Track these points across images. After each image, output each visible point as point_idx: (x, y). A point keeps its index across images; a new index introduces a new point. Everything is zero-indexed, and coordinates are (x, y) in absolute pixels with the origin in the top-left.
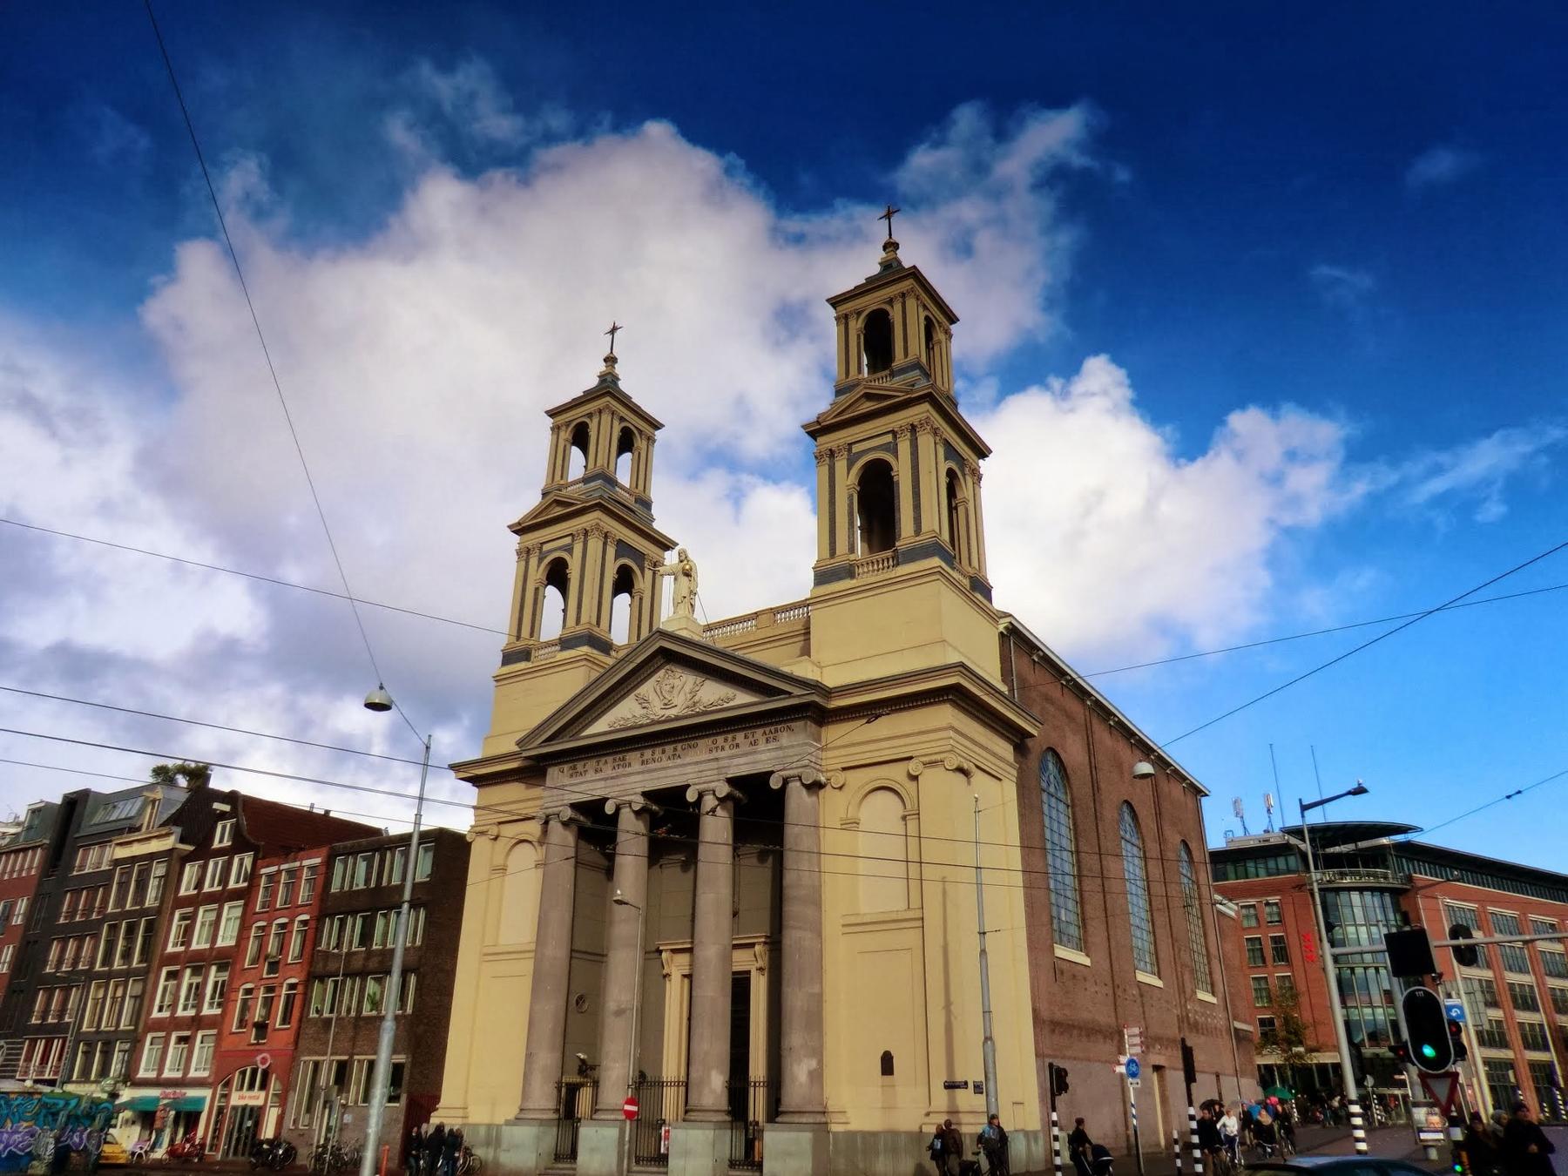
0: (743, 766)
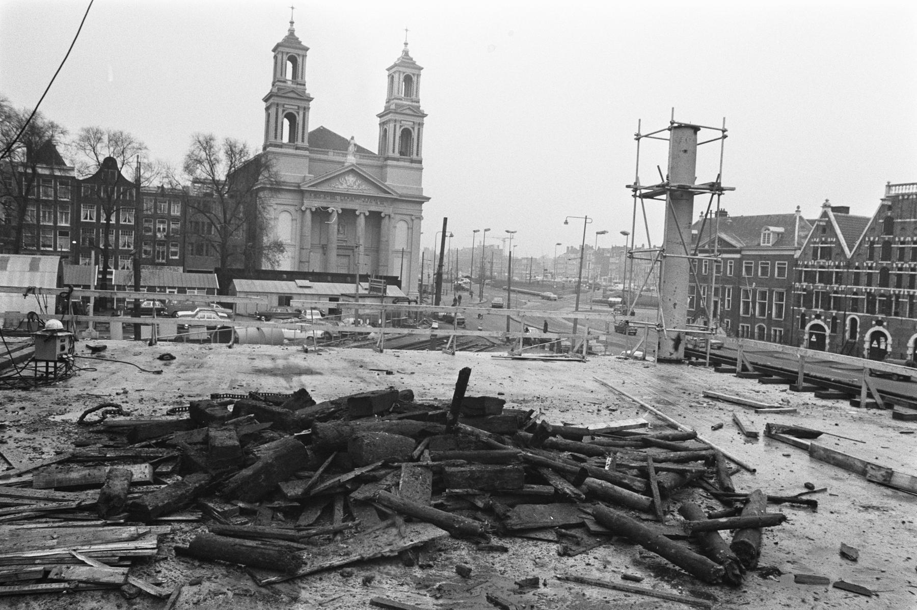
0: (374, 208)
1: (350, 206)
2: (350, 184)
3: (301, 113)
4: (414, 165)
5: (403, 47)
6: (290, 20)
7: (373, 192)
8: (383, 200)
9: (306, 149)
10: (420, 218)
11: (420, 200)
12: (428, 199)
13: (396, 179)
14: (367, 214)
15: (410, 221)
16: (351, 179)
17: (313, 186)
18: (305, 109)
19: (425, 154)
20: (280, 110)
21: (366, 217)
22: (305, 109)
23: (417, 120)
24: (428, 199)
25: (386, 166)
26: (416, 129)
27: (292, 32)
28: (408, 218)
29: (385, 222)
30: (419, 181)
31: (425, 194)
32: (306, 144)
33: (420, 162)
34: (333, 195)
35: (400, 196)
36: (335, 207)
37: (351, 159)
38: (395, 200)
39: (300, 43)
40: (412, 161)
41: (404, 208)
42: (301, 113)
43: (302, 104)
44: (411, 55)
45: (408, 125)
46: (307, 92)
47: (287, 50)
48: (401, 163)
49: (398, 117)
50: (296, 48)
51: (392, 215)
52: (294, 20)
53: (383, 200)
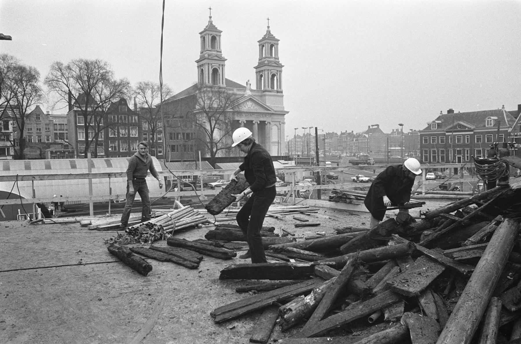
0: (262, 119)
1: (250, 119)
2: (249, 107)
3: (221, 68)
4: (279, 94)
5: (267, 29)
6: (209, 15)
7: (262, 111)
8: (265, 114)
10: (284, 123)
11: (283, 114)
12: (288, 112)
13: (270, 102)
14: (259, 122)
15: (279, 126)
16: (250, 104)
18: (222, 65)
19: (284, 88)
20: (210, 67)
22: (222, 65)
23: (279, 69)
24: (288, 112)
25: (265, 95)
27: (211, 23)
28: (278, 123)
29: (267, 127)
30: (282, 103)
31: (285, 110)
33: (282, 92)
35: (275, 112)
37: (248, 93)
38: (272, 114)
39: (216, 28)
40: (278, 92)
41: (276, 118)
42: (221, 68)
43: (221, 63)
45: (274, 72)
46: (223, 56)
47: (210, 33)
48: (272, 93)
49: (270, 68)
50: (215, 32)
51: (271, 123)
52: (211, 15)
53: (265, 114)
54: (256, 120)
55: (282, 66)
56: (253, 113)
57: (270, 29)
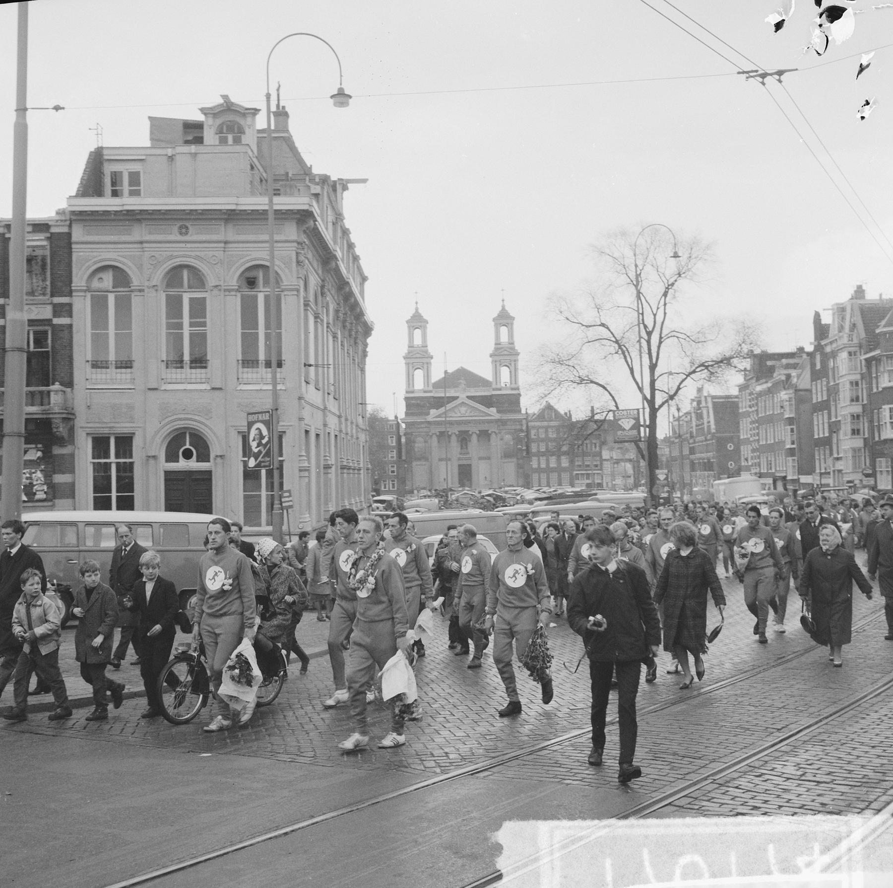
9: (431, 392)
17: (436, 417)
21: (479, 436)
23: (513, 358)
26: (513, 363)
32: (431, 388)
34: (451, 423)
36: (455, 430)
44: (507, 308)
54: (474, 429)
55: (518, 354)
56: (469, 422)
57: (505, 303)
